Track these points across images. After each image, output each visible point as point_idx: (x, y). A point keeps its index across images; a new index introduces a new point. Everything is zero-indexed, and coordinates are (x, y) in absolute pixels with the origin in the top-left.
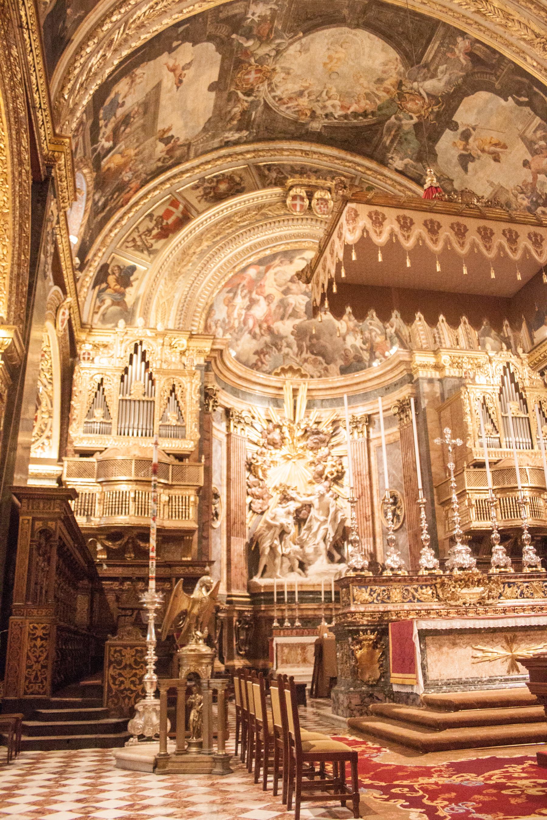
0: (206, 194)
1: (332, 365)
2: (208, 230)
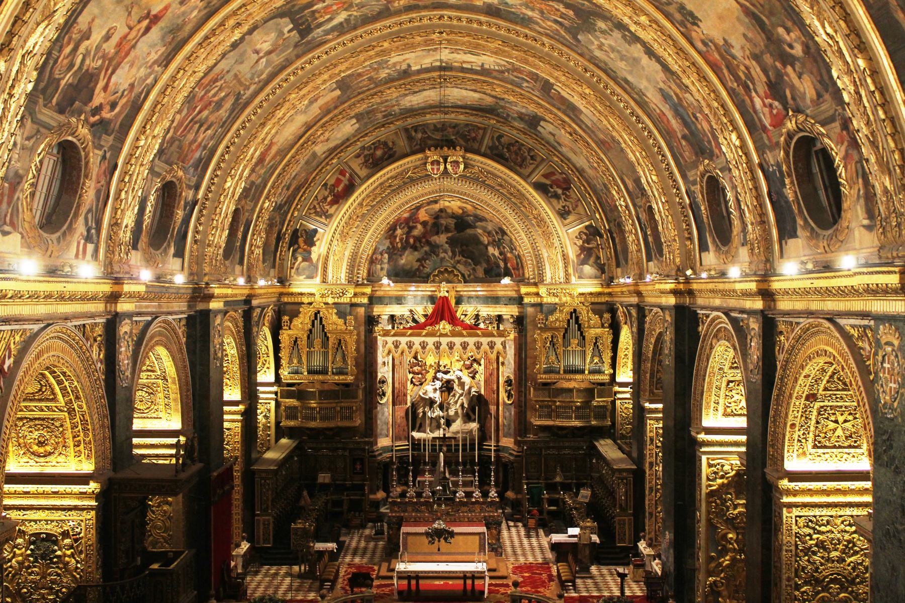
0: (366, 161)
1: (478, 267)
2: (368, 196)
